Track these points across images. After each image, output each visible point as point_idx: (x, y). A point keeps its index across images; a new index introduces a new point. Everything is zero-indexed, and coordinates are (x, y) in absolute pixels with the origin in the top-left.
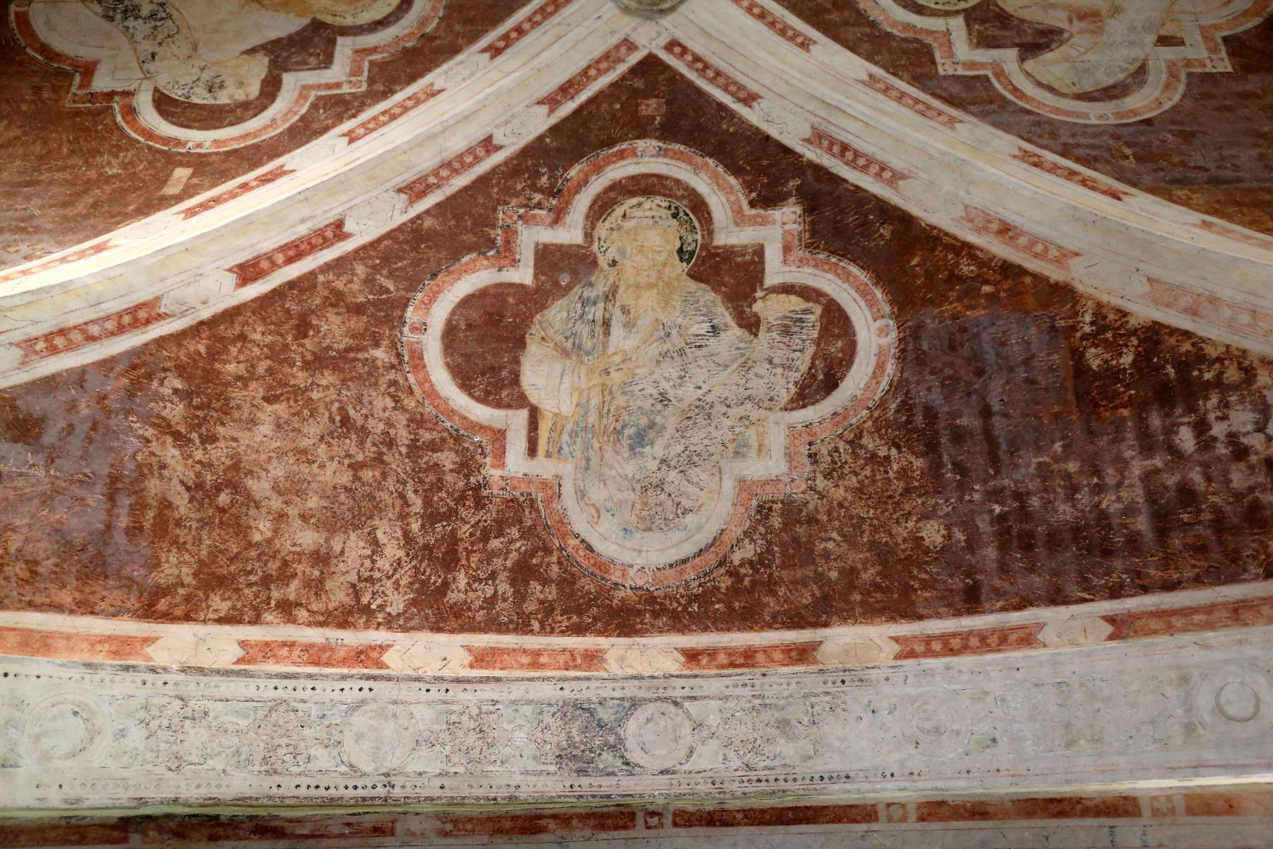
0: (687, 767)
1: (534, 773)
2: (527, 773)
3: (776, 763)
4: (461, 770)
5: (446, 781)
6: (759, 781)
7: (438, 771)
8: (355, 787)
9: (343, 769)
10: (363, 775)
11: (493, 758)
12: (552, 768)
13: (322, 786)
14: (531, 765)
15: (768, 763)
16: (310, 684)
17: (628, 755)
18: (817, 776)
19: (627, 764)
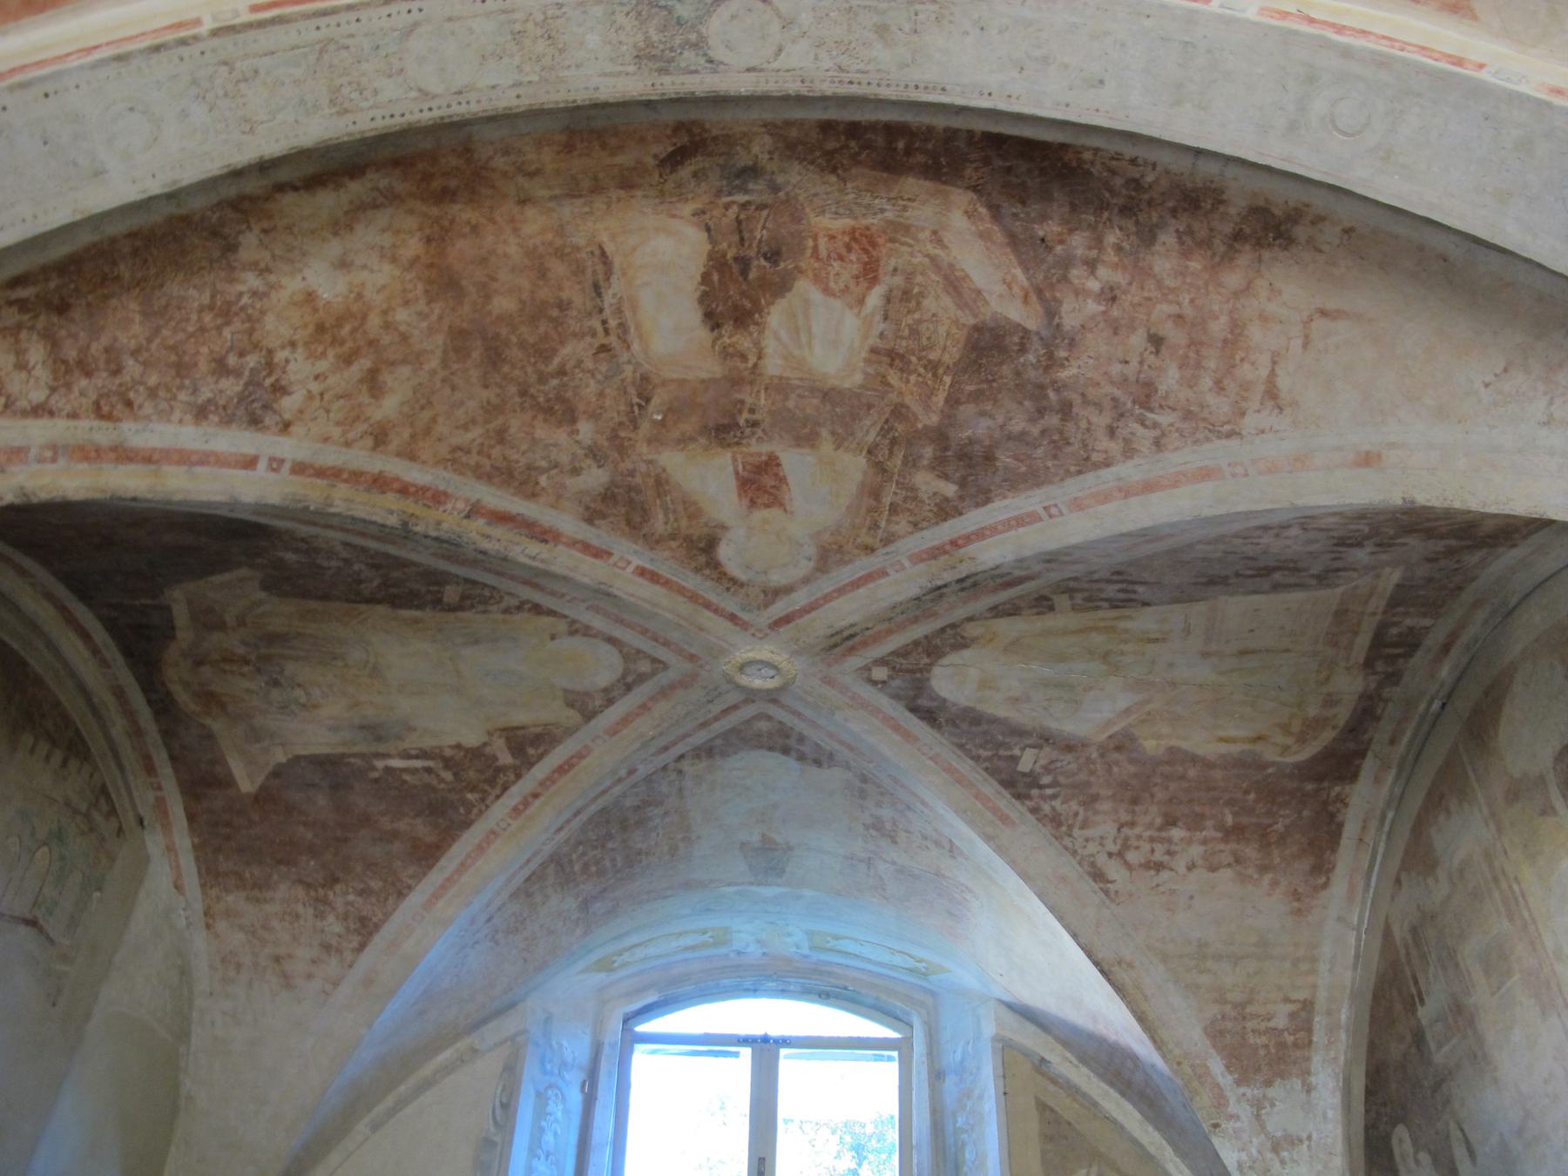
0: (775, 65)
1: (612, 75)
2: (605, 75)
3: (869, 67)
4: (535, 78)
5: (521, 91)
6: (851, 83)
7: (511, 83)
8: (430, 109)
9: (414, 94)
10: (435, 97)
11: (567, 63)
12: (631, 69)
13: (397, 114)
14: (609, 68)
15: (861, 66)
16: (353, 16)
17: (711, 53)
18: (912, 85)
19: (711, 61)
